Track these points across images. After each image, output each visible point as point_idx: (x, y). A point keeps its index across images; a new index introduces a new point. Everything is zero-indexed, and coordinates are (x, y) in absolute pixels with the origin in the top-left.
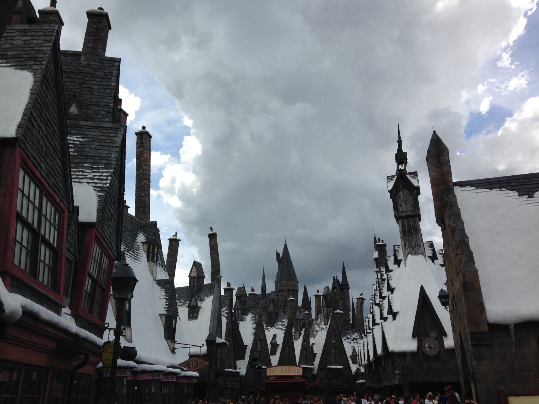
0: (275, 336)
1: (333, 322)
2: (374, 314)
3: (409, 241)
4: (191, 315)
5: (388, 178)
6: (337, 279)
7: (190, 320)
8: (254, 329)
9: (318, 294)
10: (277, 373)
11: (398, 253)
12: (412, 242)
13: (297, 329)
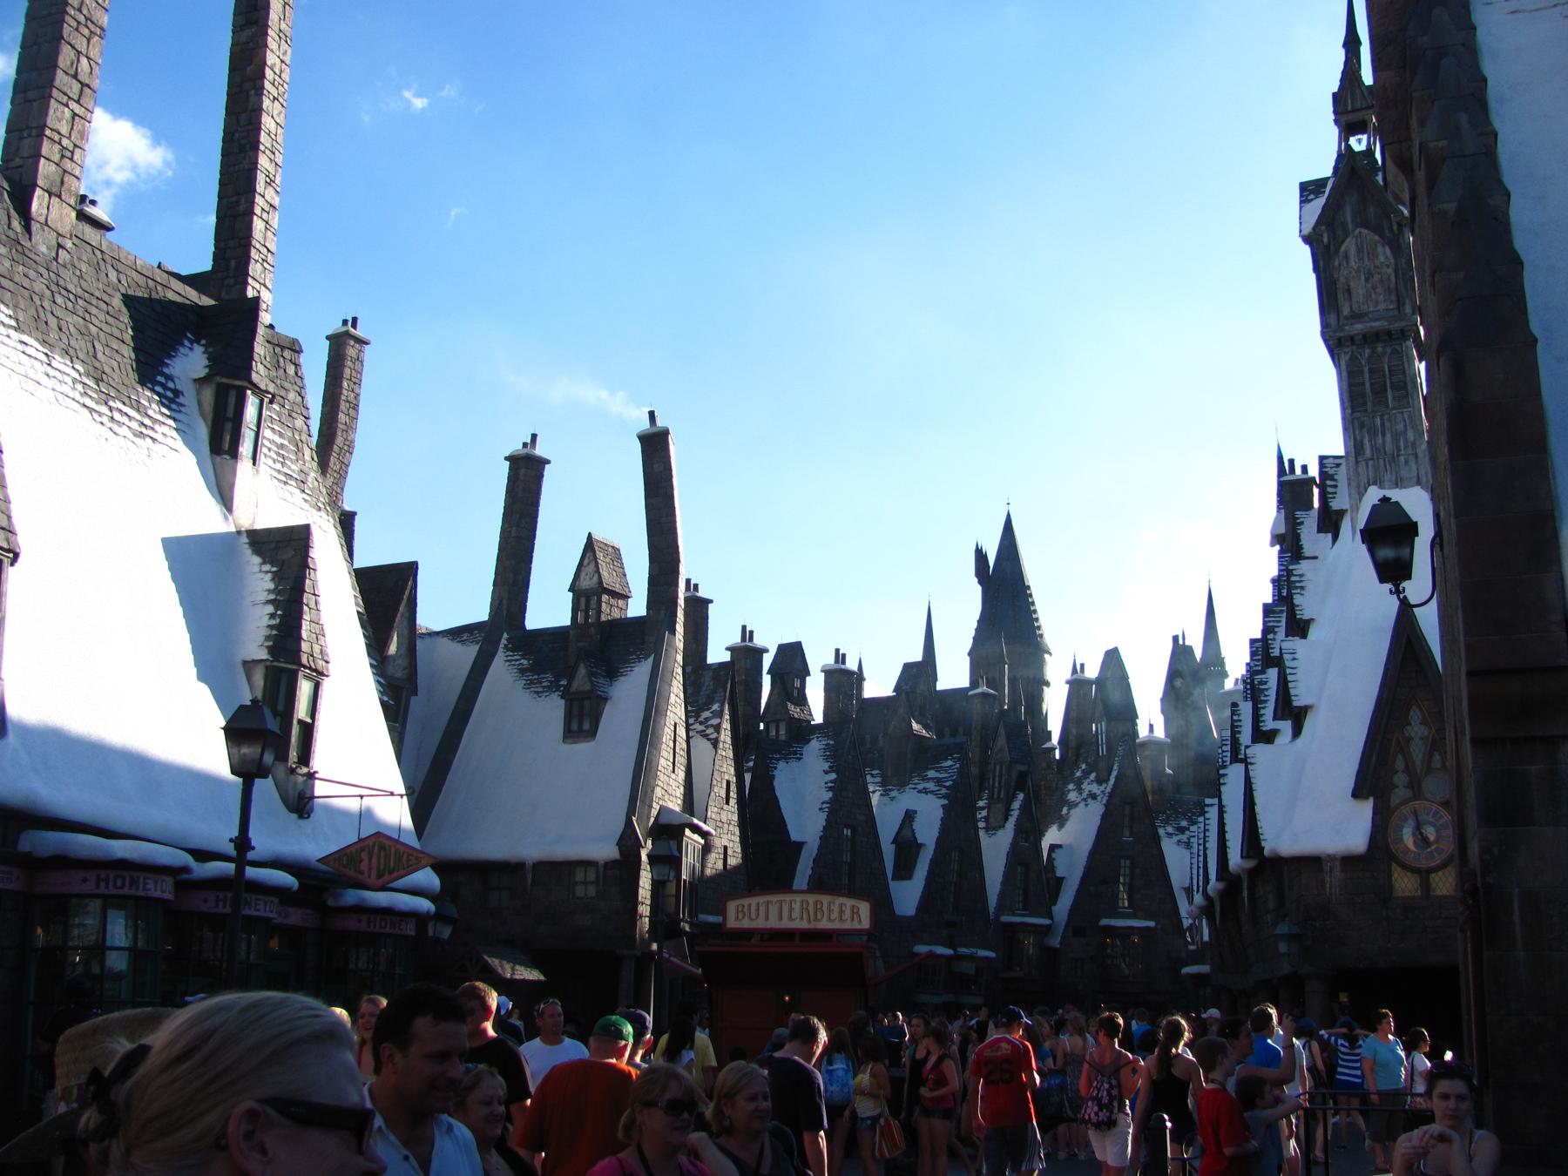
0: (909, 816)
2: (1237, 726)
3: (1373, 432)
4: (575, 727)
5: (1304, 187)
6: (1187, 644)
8: (830, 789)
10: (767, 918)
11: (1336, 486)
12: (1384, 435)
13: (996, 796)
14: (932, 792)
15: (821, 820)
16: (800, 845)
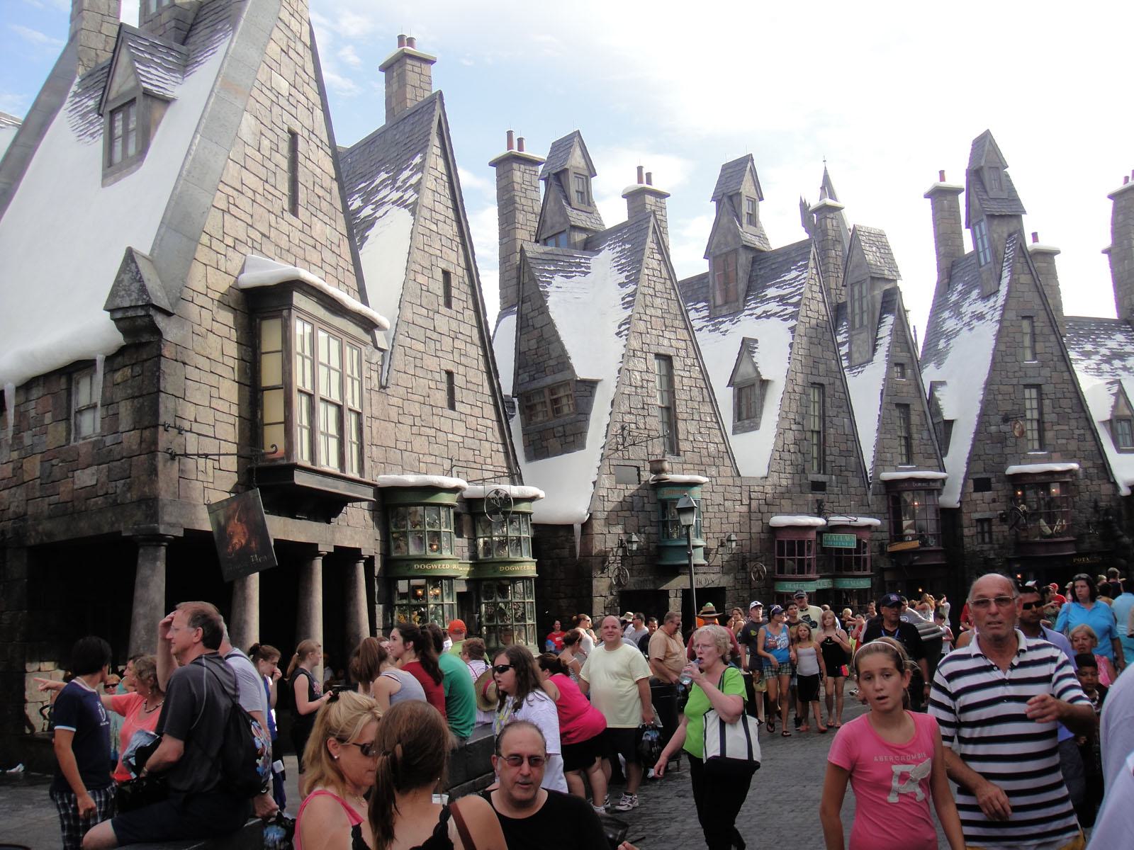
0: (748, 346)
1: (1025, 279)
7: (112, 179)
9: (943, 184)
14: (774, 314)
16: (590, 386)
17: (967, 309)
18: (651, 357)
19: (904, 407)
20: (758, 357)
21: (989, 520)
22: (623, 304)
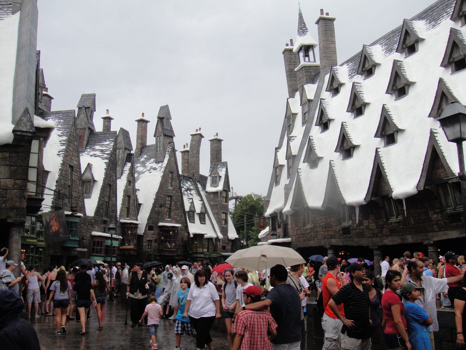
0: (89, 166)
1: (173, 159)
14: (99, 156)
15: (59, 160)
17: (148, 164)
18: (68, 165)
19: (129, 197)
20: (93, 171)
21: (151, 241)
22: (61, 143)
